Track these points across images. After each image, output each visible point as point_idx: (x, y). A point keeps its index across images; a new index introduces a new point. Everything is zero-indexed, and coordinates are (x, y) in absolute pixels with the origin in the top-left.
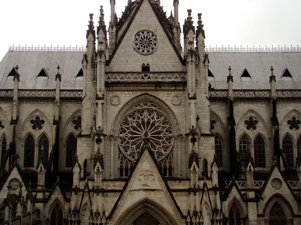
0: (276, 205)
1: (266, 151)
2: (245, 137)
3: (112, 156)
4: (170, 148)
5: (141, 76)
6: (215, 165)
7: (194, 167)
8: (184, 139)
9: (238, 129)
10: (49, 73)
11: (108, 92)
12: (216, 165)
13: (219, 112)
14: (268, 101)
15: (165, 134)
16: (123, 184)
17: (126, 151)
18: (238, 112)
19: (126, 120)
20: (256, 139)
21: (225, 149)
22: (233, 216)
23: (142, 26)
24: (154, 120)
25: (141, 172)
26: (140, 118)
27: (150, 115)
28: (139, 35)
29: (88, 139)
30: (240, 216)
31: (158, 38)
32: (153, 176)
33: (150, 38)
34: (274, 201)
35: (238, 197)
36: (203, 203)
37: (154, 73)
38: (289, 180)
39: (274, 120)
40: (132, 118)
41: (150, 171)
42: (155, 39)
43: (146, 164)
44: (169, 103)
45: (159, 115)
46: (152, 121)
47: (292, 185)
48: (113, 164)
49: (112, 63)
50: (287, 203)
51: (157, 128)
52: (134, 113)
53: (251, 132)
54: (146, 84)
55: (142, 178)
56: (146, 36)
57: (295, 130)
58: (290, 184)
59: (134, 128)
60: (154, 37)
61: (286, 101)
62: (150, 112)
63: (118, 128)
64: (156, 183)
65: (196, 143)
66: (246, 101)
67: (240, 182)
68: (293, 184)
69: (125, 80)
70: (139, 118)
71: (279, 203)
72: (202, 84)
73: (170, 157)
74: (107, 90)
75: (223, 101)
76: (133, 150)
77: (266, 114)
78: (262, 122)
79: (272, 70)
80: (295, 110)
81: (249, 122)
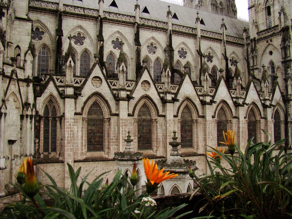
0: (95, 104)
9: (66, 42)
12: (31, 54)
13: (49, 23)
14: (96, 20)
18: (67, 26)
20: (82, 54)
21: (52, 60)
22: (49, 115)
34: (93, 99)
35: (55, 93)
38: (110, 79)
39: (100, 37)
47: (112, 85)
50: (106, 102)
57: (117, 50)
58: (110, 84)
61: (111, 22)
66: (76, 17)
68: (113, 84)
71: (98, 102)
75: (53, 14)
77: (93, 32)
80: (118, 32)
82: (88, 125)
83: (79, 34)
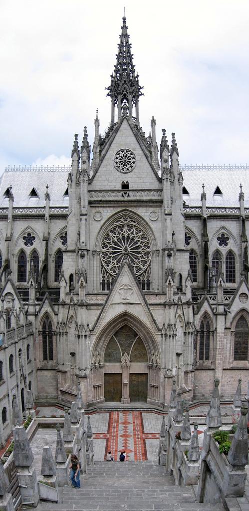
2: (217, 252)
3: (95, 271)
4: (148, 263)
5: (121, 194)
7: (170, 281)
8: (161, 253)
10: (38, 192)
15: (143, 249)
16: (105, 298)
17: (108, 266)
19: (108, 235)
23: (122, 145)
24: (133, 235)
26: (120, 233)
27: (130, 230)
28: (119, 154)
29: (73, 254)
31: (136, 157)
32: (132, 290)
33: (129, 157)
36: (177, 317)
37: (133, 191)
42: (134, 158)
43: (126, 278)
45: (138, 230)
48: (95, 279)
49: (94, 182)
52: (114, 229)
53: (223, 248)
56: (125, 155)
59: (116, 244)
60: (133, 156)
62: (130, 227)
63: (100, 243)
64: (135, 296)
65: (172, 258)
67: (211, 296)
70: (119, 233)
76: (114, 264)
79: (241, 187)
82: (235, 337)
83: (223, 235)
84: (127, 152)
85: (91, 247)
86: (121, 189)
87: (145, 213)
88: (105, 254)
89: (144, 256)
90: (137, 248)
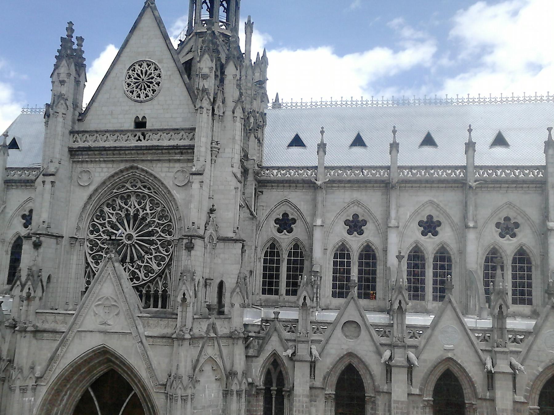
1: (378, 271)
6: (238, 293)
9: (332, 233)
11: (74, 165)
13: (302, 203)
15: (160, 236)
17: (97, 263)
19: (102, 211)
24: (145, 212)
25: (99, 300)
27: (140, 203)
28: (134, 70)
30: (283, 385)
40: (111, 208)
41: (112, 298)
44: (169, 183)
46: (141, 214)
49: (89, 117)
51: (149, 225)
52: (114, 200)
54: (133, 150)
55: (100, 311)
57: (430, 237)
62: (141, 197)
63: (85, 225)
69: (101, 144)
70: (121, 208)
72: (227, 150)
73: (166, 275)
74: (74, 162)
78: (374, 223)
80: (431, 202)
81: (352, 221)
84: (148, 65)
85: (67, 228)
86: (132, 126)
87: (166, 173)
88: (93, 244)
89: (161, 249)
90: (151, 234)
